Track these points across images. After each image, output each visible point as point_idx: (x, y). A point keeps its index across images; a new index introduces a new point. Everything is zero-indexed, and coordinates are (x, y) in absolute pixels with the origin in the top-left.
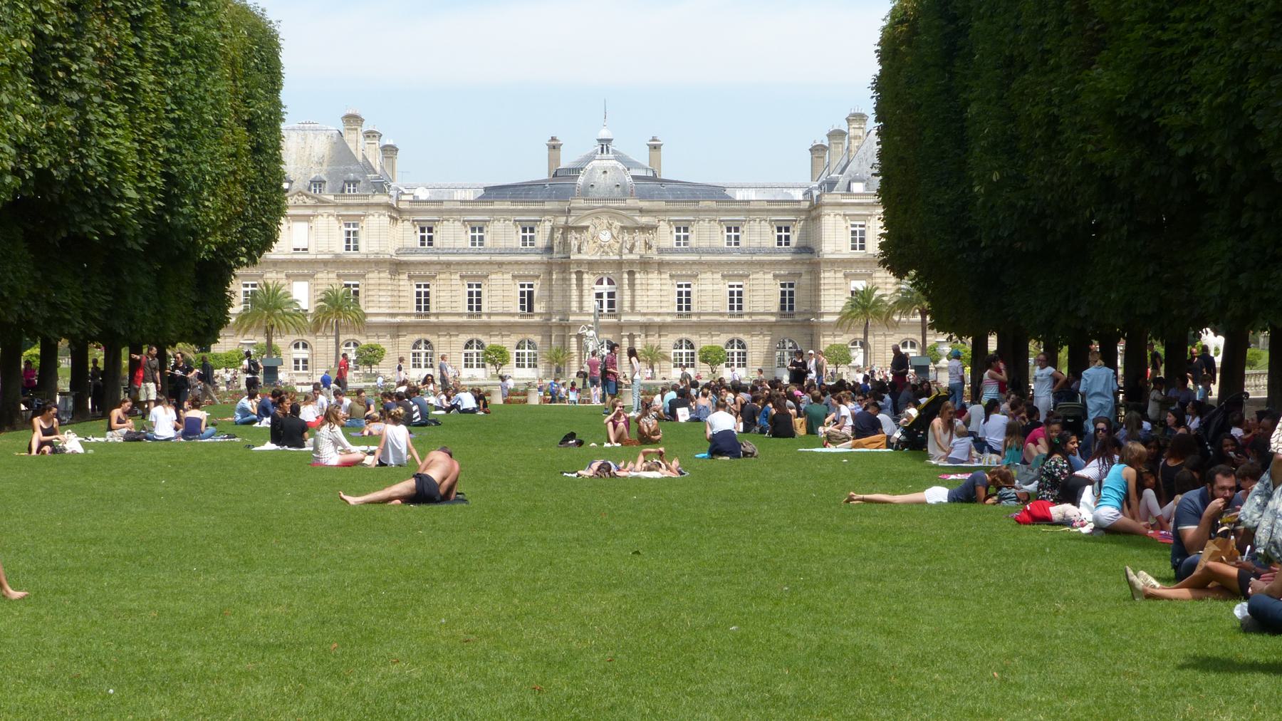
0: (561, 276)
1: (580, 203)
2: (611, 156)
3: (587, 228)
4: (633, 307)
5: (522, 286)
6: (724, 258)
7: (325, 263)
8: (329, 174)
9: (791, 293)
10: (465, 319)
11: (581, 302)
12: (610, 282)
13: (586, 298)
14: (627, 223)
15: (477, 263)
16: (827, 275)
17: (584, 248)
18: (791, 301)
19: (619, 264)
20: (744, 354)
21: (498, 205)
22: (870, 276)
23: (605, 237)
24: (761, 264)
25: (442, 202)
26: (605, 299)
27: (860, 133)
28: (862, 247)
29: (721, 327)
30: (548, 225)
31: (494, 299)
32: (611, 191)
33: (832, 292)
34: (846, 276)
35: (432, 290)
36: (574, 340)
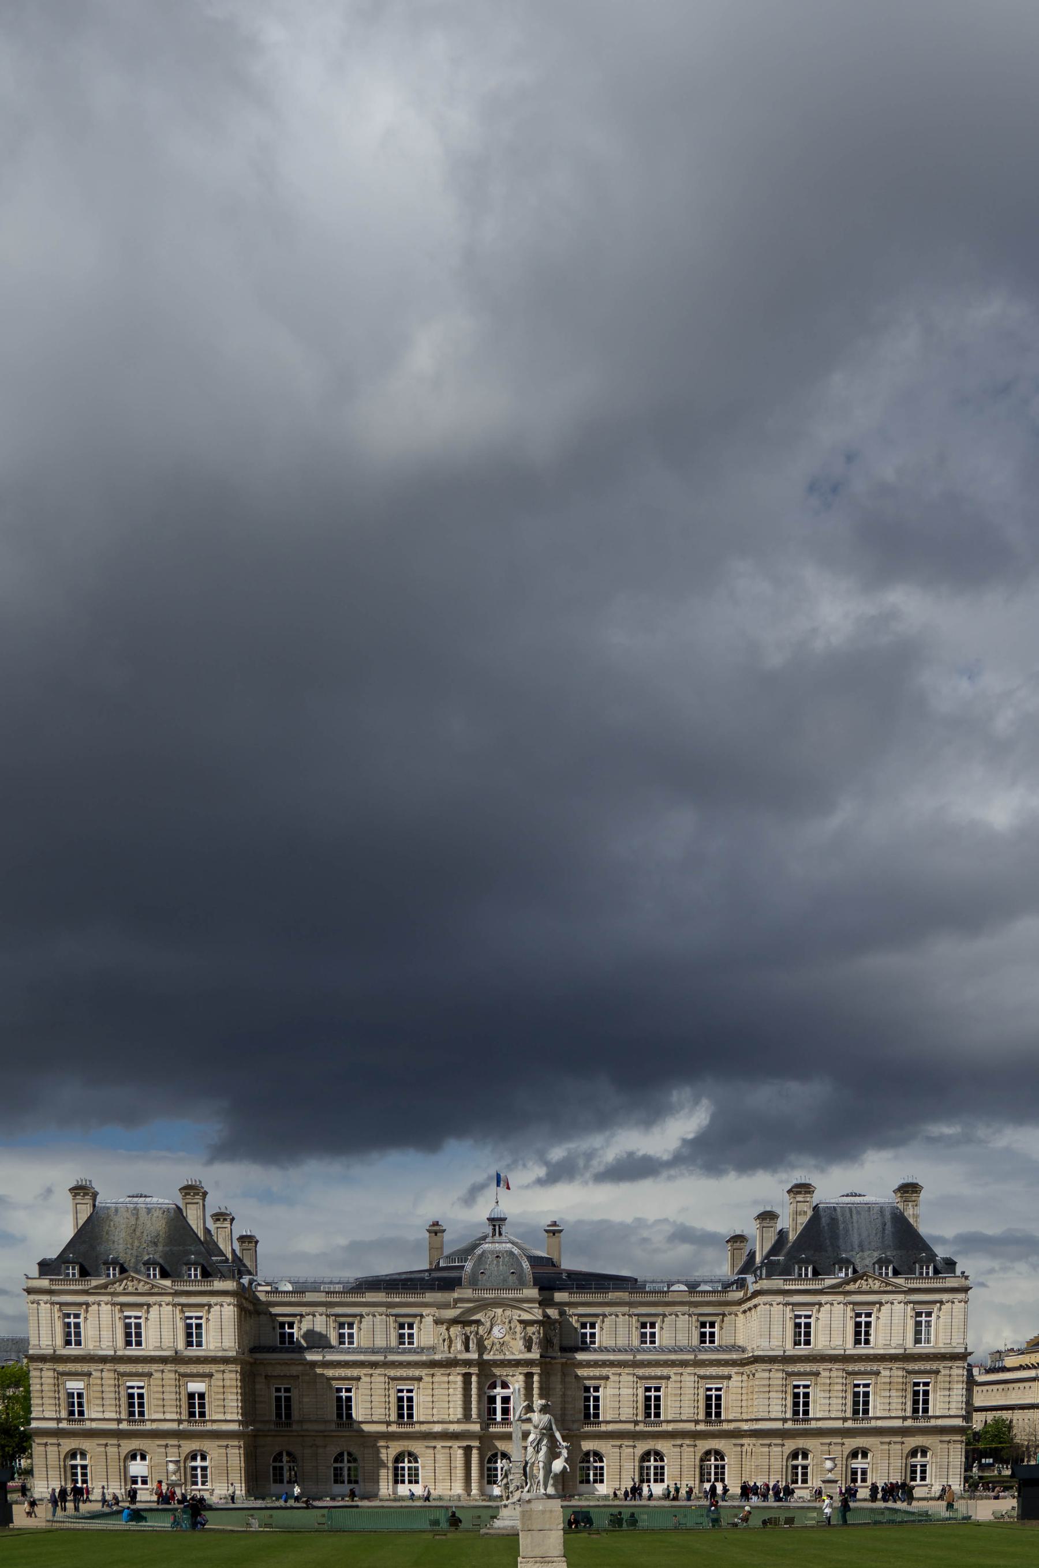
0: (445, 1379)
1: (468, 1293)
2: (503, 1238)
3: (478, 1322)
7: (164, 1360)
9: (718, 1398)
12: (505, 1385)
16: (766, 1375)
17: (472, 1346)
18: (718, 1406)
19: (517, 1363)
20: (662, 1468)
21: (370, 1297)
24: (684, 1364)
26: (499, 1406)
28: (808, 1343)
30: (429, 1320)
32: (505, 1280)
35: (294, 1394)
36: (460, 1452)
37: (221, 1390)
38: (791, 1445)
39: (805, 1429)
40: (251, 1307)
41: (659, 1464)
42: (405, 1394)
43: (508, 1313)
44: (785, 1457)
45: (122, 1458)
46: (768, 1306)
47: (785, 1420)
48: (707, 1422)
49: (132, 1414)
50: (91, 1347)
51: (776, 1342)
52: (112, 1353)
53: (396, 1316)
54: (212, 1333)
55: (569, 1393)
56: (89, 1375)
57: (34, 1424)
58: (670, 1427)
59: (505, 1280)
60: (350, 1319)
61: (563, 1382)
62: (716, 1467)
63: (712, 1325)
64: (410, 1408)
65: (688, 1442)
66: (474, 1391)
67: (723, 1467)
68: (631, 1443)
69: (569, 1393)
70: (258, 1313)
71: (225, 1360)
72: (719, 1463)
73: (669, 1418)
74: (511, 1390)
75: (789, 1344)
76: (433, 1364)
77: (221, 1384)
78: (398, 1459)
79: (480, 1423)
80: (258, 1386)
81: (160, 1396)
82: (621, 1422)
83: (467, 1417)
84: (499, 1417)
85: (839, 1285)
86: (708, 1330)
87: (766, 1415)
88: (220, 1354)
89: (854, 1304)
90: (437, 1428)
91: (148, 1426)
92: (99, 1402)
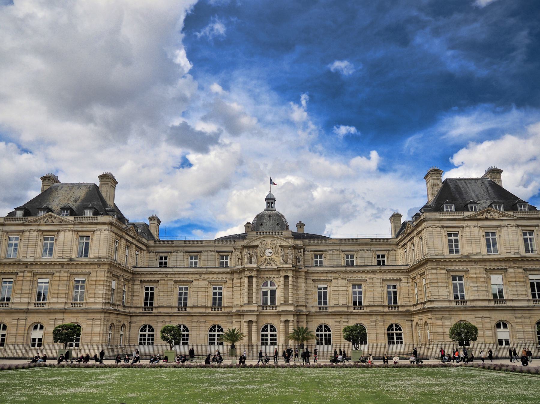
0: (239, 281)
3: (257, 247)
5: (215, 289)
6: (349, 268)
7: (62, 264)
8: (78, 208)
9: (395, 293)
11: (250, 297)
12: (272, 284)
13: (254, 295)
14: (284, 244)
16: (434, 271)
18: (395, 298)
19: (279, 270)
22: (467, 271)
24: (374, 272)
25: (173, 241)
27: (438, 182)
28: (457, 251)
29: (348, 314)
31: (196, 297)
32: (273, 228)
33: (440, 284)
35: (155, 291)
36: (246, 324)
37: (94, 283)
39: (465, 307)
40: (144, 248)
42: (217, 291)
43: (274, 242)
45: (27, 328)
47: (450, 301)
48: (390, 307)
49: (39, 299)
50: (21, 257)
51: (437, 251)
52: (33, 260)
53: (219, 252)
54: (93, 248)
55: (309, 289)
56: (17, 273)
58: (368, 310)
60: (196, 254)
61: (306, 283)
62: (397, 334)
63: (383, 256)
64: (220, 299)
65: (379, 318)
66: (254, 287)
67: (401, 334)
68: (346, 320)
71: (99, 264)
72: (398, 332)
73: (368, 305)
74: (276, 287)
75: (446, 253)
76: (232, 273)
77: (94, 279)
78: (212, 329)
79: (258, 306)
80: (135, 287)
81: (57, 287)
82: (340, 306)
83: (250, 303)
84: (269, 303)
86: (381, 259)
89: (485, 227)
90: (234, 310)
91: (47, 306)
92: (19, 291)
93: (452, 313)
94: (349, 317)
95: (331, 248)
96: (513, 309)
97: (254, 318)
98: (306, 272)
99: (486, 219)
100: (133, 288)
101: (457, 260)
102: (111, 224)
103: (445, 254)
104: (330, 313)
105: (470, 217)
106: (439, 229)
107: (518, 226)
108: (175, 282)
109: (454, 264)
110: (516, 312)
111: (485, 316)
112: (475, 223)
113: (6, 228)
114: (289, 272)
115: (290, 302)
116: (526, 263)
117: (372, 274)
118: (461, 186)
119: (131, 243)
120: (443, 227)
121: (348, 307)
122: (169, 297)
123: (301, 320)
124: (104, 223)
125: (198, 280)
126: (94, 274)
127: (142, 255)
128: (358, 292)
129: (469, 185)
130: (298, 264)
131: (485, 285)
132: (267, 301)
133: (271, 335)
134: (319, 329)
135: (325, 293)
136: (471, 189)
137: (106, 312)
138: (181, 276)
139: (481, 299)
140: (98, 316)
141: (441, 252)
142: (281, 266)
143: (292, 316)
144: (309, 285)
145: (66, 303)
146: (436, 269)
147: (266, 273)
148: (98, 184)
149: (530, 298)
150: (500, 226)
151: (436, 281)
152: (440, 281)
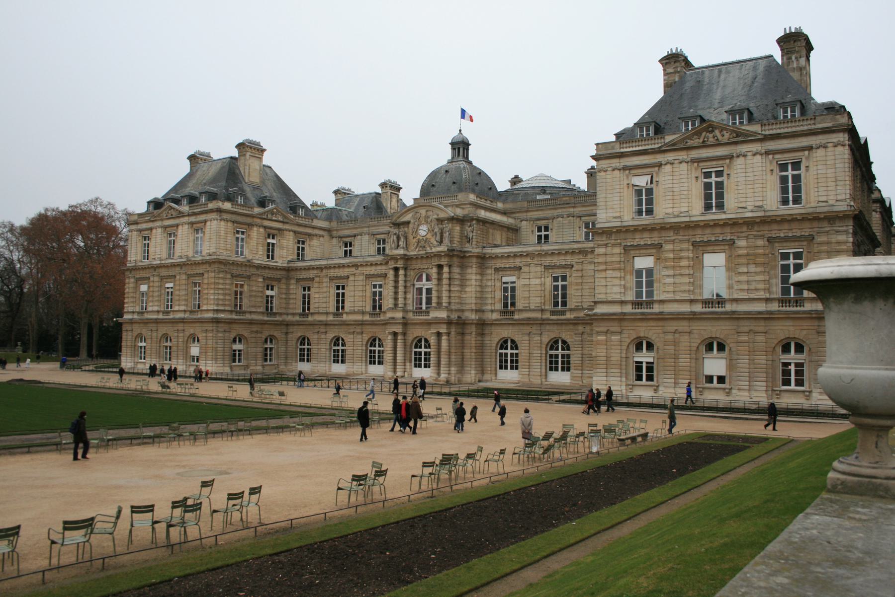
3: (408, 223)
4: (439, 304)
5: (375, 286)
10: (331, 318)
12: (428, 279)
13: (401, 295)
14: (442, 215)
15: (339, 266)
16: (602, 250)
17: (401, 243)
20: (569, 356)
22: (659, 246)
23: (423, 230)
28: (650, 212)
32: (449, 190)
33: (610, 273)
34: (627, 249)
36: (390, 337)
38: (630, 333)
39: (643, 314)
40: (321, 233)
41: (566, 352)
42: (378, 290)
43: (430, 213)
44: (624, 347)
46: (603, 174)
47: (622, 302)
55: (489, 284)
57: (127, 317)
59: (449, 190)
60: (382, 236)
66: (401, 283)
69: (489, 284)
70: (332, 237)
73: (573, 307)
77: (206, 281)
79: (405, 311)
80: (292, 287)
82: (530, 310)
83: (396, 305)
84: (424, 308)
85: (683, 140)
87: (602, 297)
88: (208, 258)
93: (625, 323)
94: (543, 327)
95: (559, 211)
96: (733, 317)
97: (399, 329)
98: (483, 259)
99: (704, 145)
100: (288, 289)
101: (640, 228)
102: (219, 211)
103: (626, 218)
104: (519, 320)
105: (674, 145)
106: (617, 172)
107: (767, 153)
108: (332, 279)
109: (638, 236)
110: (742, 323)
111: (680, 328)
112: (682, 155)
113: (140, 227)
114: (443, 259)
115: (444, 304)
116: (775, 226)
117: (581, 256)
118: (707, 80)
119: (279, 230)
120: (625, 168)
121: (542, 311)
122: (325, 300)
123: (468, 331)
124: (212, 211)
125: (354, 274)
126: (206, 275)
127: (315, 242)
128: (562, 286)
129: (723, 76)
130: (467, 245)
131: (687, 272)
132: (421, 304)
133: (426, 353)
134: (503, 345)
135: (513, 289)
136: (721, 83)
137: (217, 321)
138: (337, 270)
139: (678, 298)
140: (209, 326)
141: (618, 214)
142: (434, 250)
143: (445, 326)
144: (489, 277)
145: (185, 311)
146: (606, 245)
147: (419, 261)
148: (237, 156)
149: (779, 295)
150: (731, 157)
151: (603, 267)
152: (611, 267)
